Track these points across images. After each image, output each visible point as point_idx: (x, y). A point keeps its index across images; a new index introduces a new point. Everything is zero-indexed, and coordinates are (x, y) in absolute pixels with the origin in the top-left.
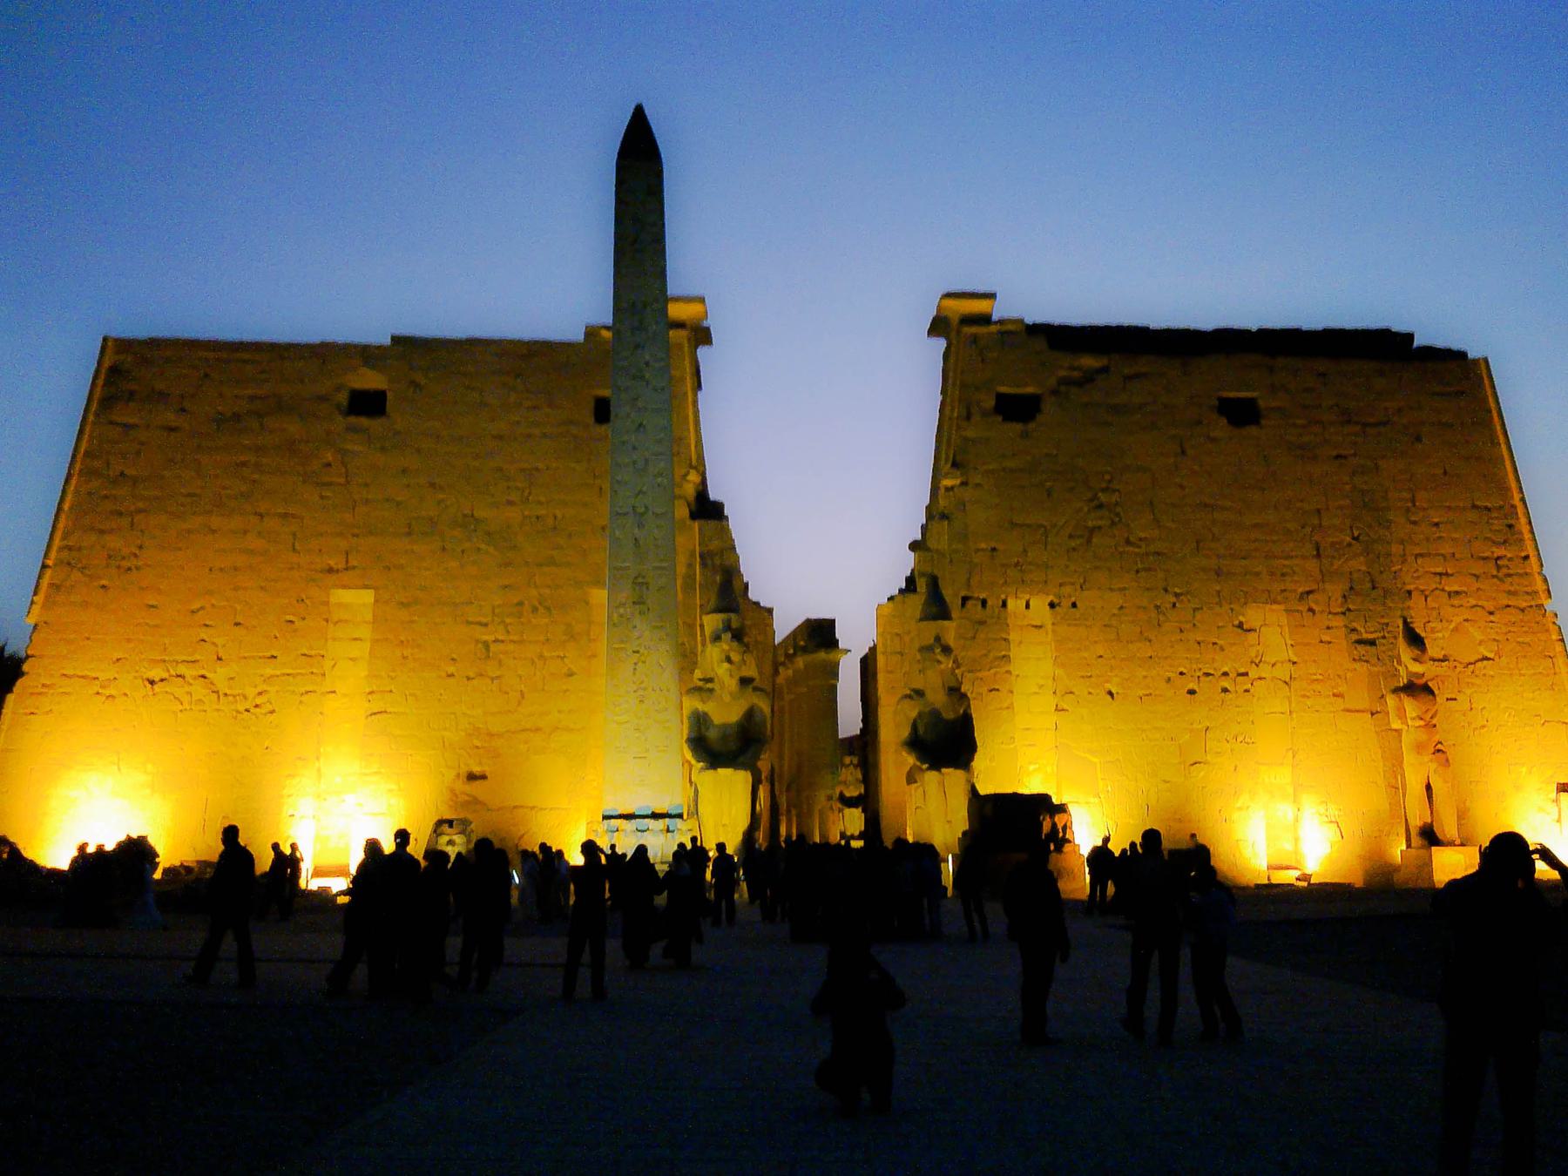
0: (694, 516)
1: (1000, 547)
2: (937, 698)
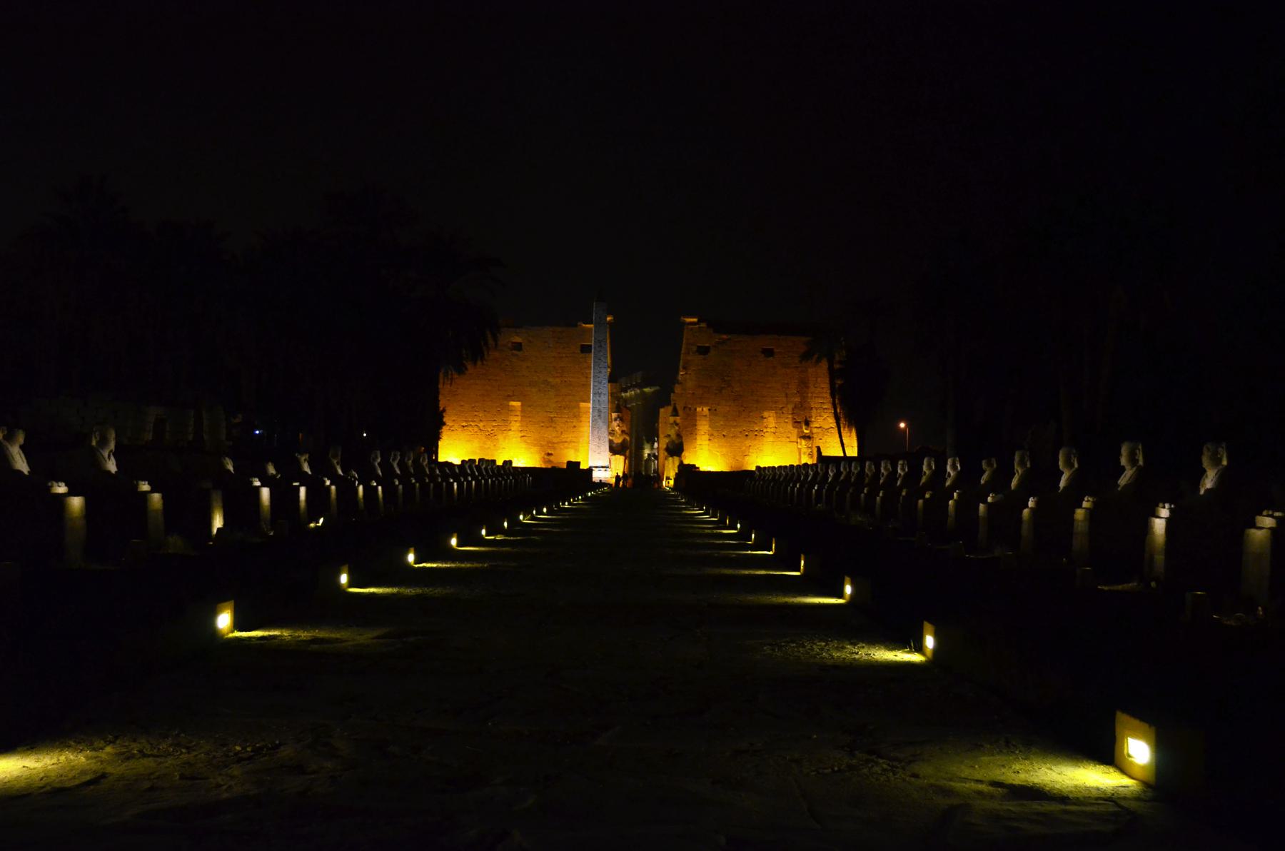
2: (674, 436)
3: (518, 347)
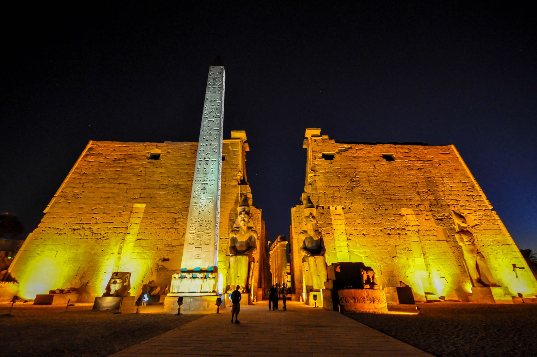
1: (327, 192)
2: (311, 233)
3: (156, 157)
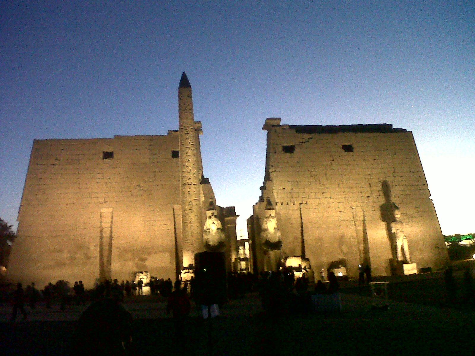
0: (201, 183)
